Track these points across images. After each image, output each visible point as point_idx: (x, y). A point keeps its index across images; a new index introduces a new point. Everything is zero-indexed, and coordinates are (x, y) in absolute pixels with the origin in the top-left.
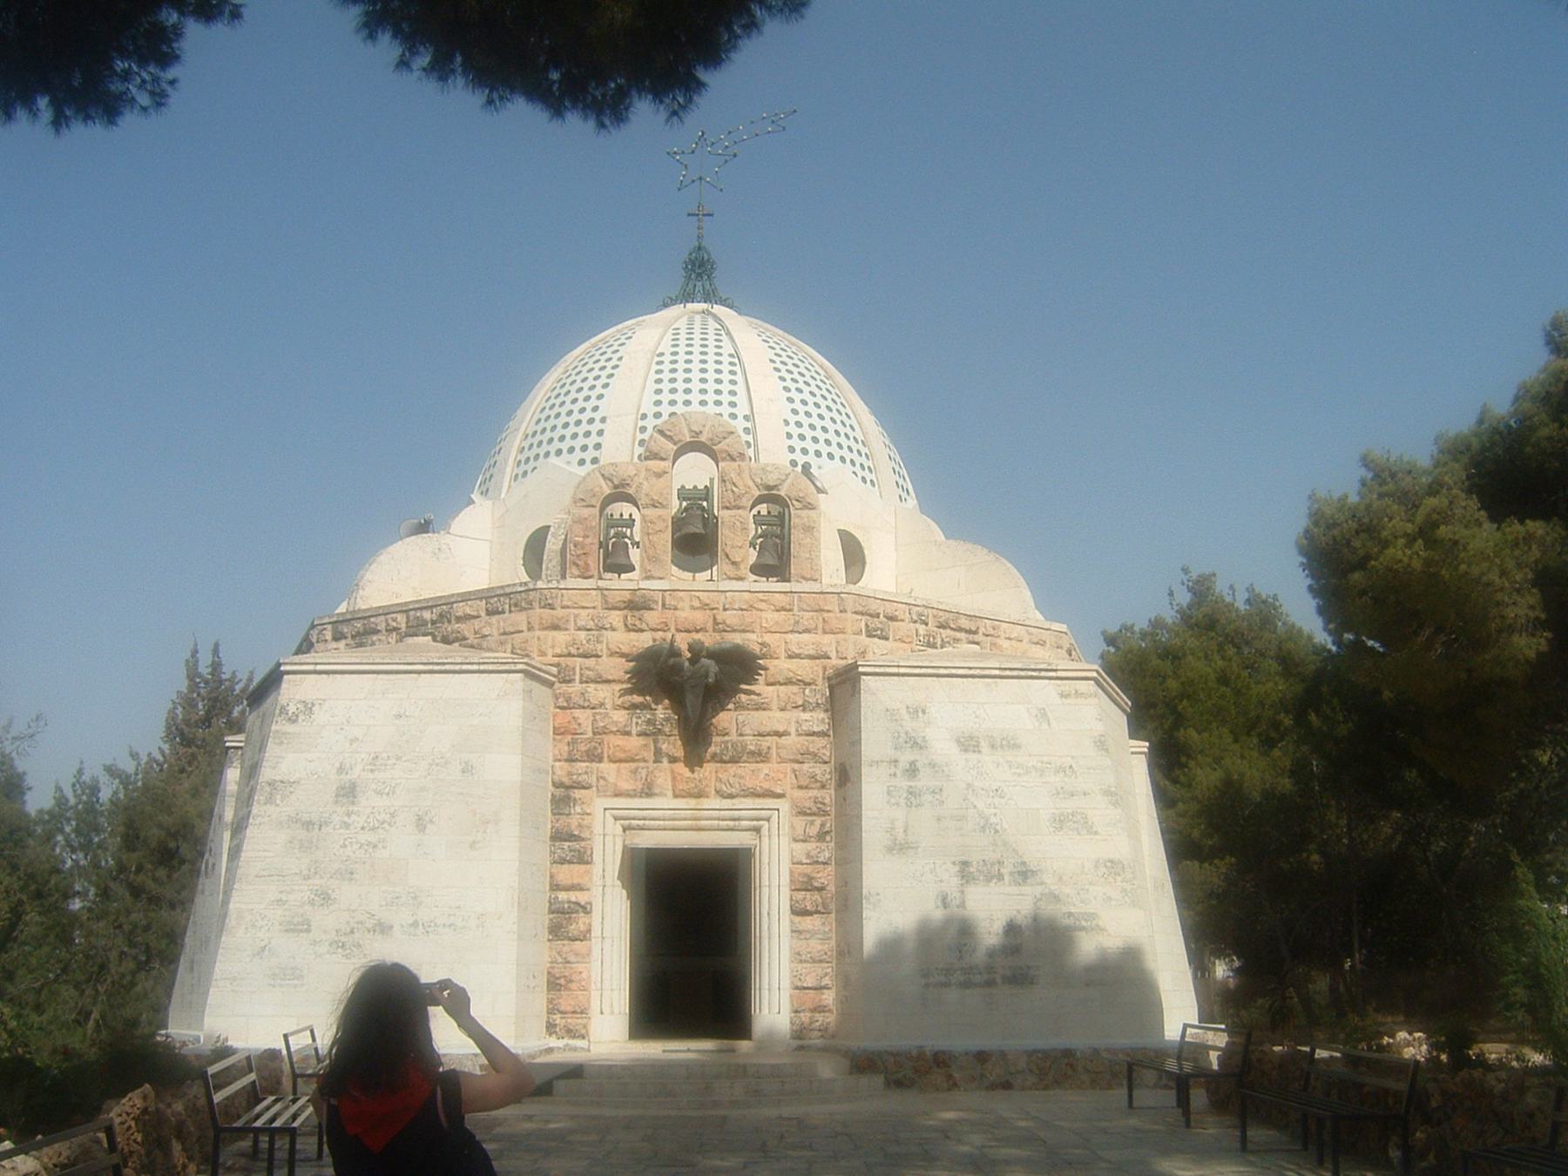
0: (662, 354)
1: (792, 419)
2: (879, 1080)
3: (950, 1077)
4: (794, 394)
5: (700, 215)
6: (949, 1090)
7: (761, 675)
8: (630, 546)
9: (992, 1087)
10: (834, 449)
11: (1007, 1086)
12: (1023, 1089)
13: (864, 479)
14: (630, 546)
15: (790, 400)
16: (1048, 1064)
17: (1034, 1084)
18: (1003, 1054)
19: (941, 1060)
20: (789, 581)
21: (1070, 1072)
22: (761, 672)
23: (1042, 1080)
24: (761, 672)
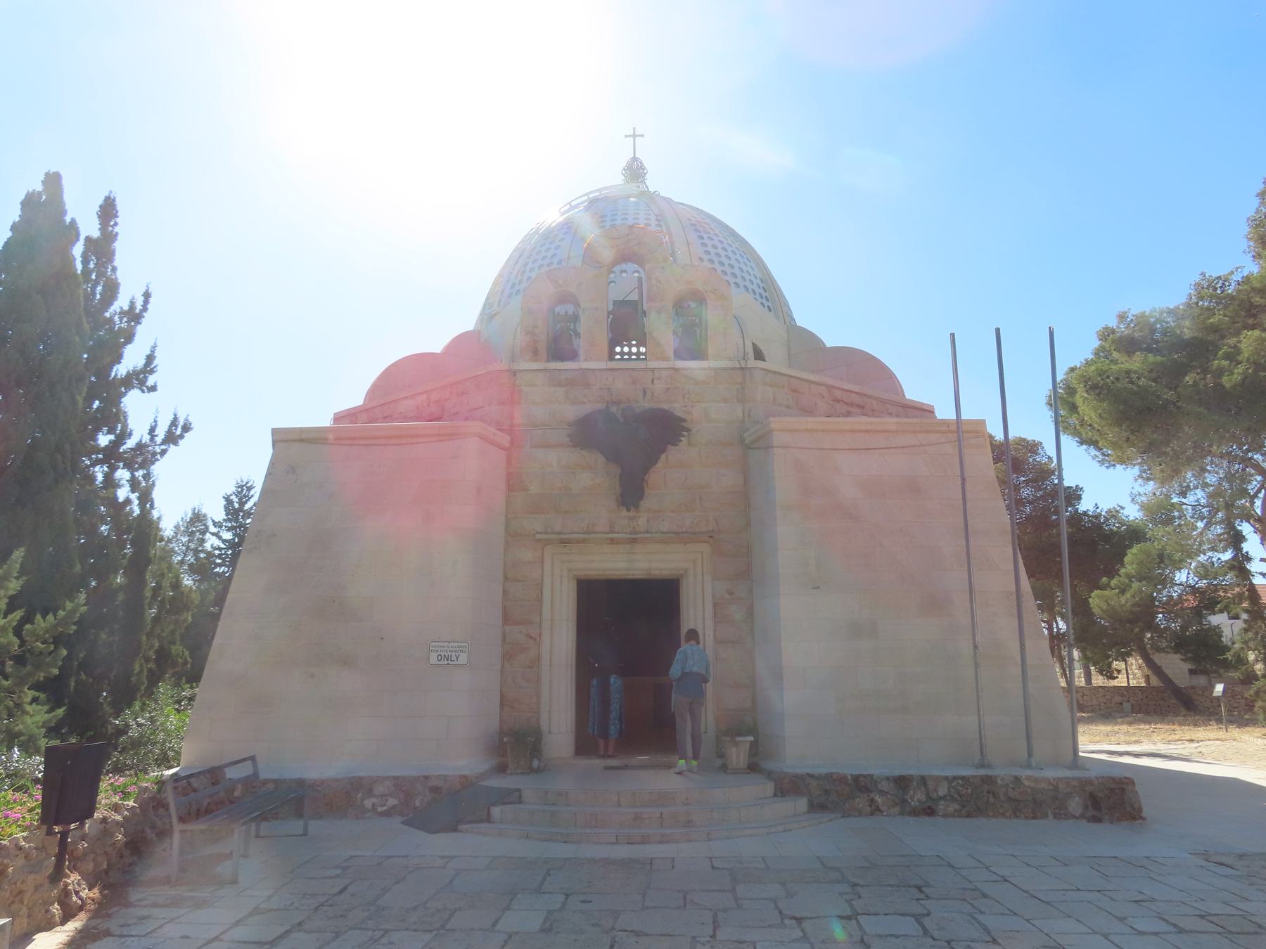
0: (605, 216)
1: (706, 257)
2: (802, 804)
3: (872, 801)
4: (706, 241)
5: (634, 136)
6: (872, 814)
7: (684, 436)
8: (574, 337)
9: (915, 813)
10: (739, 280)
11: (930, 811)
12: (945, 816)
13: (762, 303)
14: (574, 337)
15: (704, 245)
16: (969, 791)
17: (956, 811)
18: (923, 780)
19: (862, 785)
20: (707, 359)
21: (992, 799)
22: (684, 433)
23: (964, 806)
24: (684, 433)
